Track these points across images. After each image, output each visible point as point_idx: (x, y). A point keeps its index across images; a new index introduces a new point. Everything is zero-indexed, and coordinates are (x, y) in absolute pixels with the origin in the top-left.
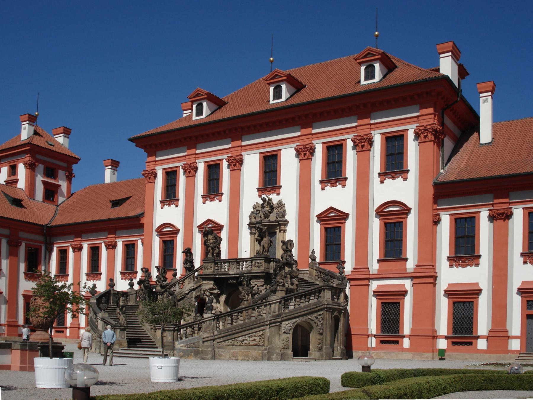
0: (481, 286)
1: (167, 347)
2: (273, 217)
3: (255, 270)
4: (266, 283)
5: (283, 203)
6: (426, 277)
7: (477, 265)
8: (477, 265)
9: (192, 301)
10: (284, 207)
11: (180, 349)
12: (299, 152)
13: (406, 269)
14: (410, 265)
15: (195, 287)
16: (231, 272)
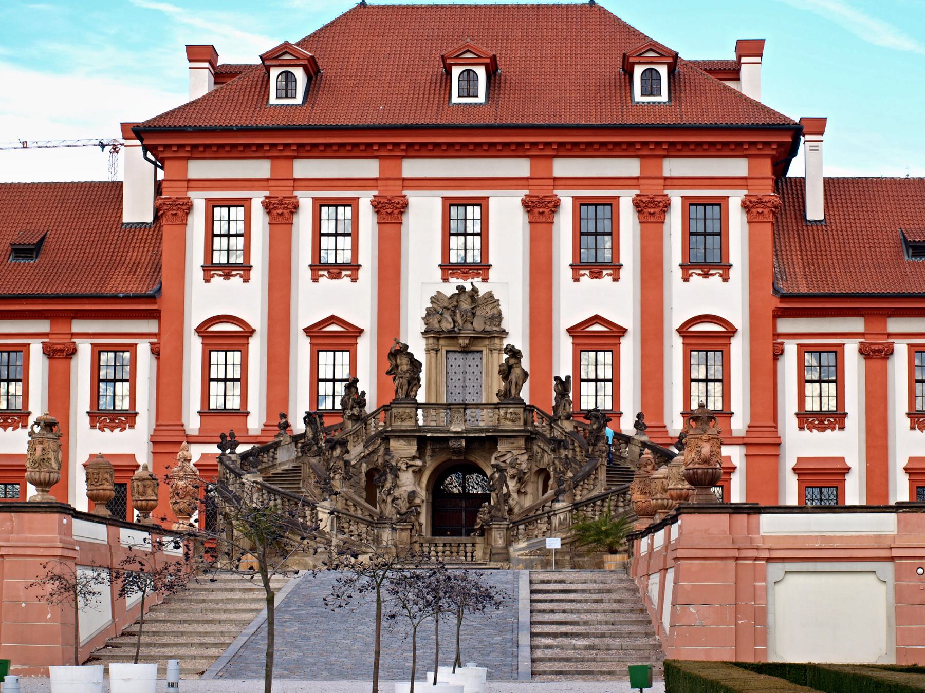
0: (849, 462)
1: (497, 557)
2: (478, 325)
3: (508, 425)
4: (528, 449)
5: (496, 297)
6: (764, 444)
7: (842, 428)
8: (842, 428)
9: (360, 479)
10: (499, 305)
11: (518, 560)
12: (528, 206)
13: (731, 431)
14: (739, 424)
15: (367, 452)
16: (454, 428)
